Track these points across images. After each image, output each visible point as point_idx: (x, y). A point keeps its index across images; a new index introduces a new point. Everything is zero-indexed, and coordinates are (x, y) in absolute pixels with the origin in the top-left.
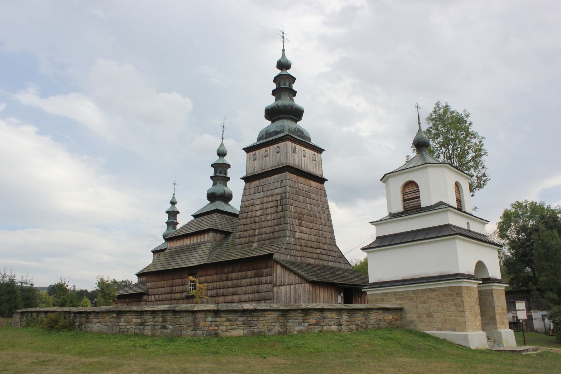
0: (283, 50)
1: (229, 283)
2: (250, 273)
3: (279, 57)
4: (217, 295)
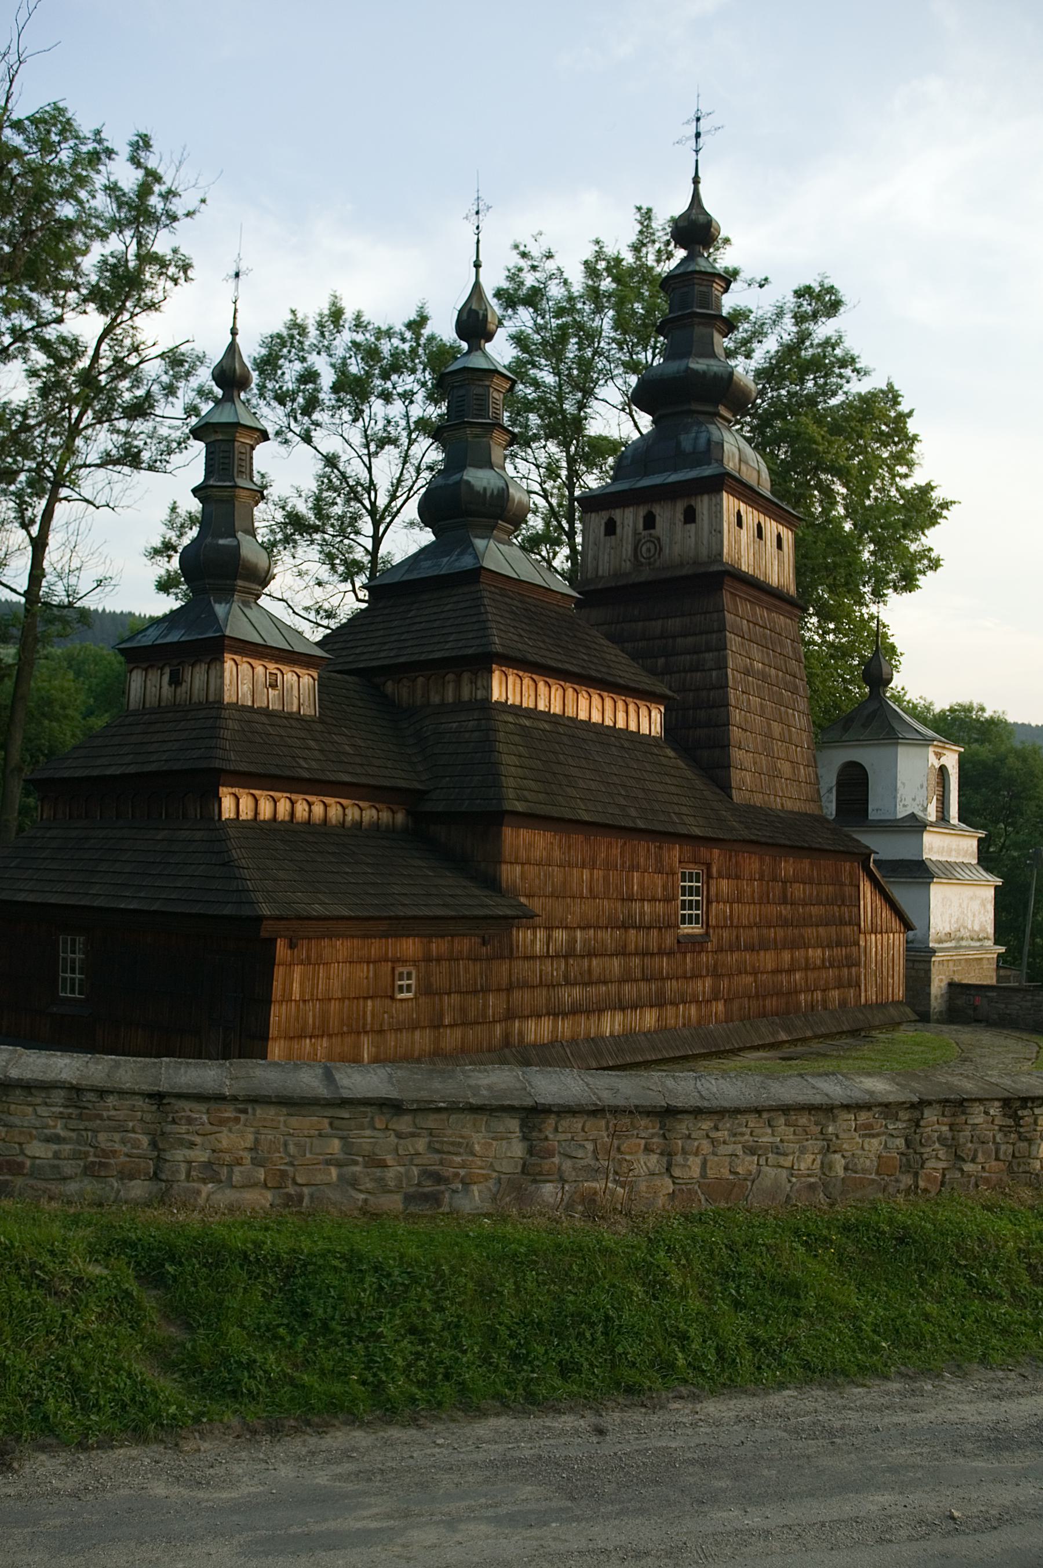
0: (696, 181)
1: (786, 911)
4: (764, 946)
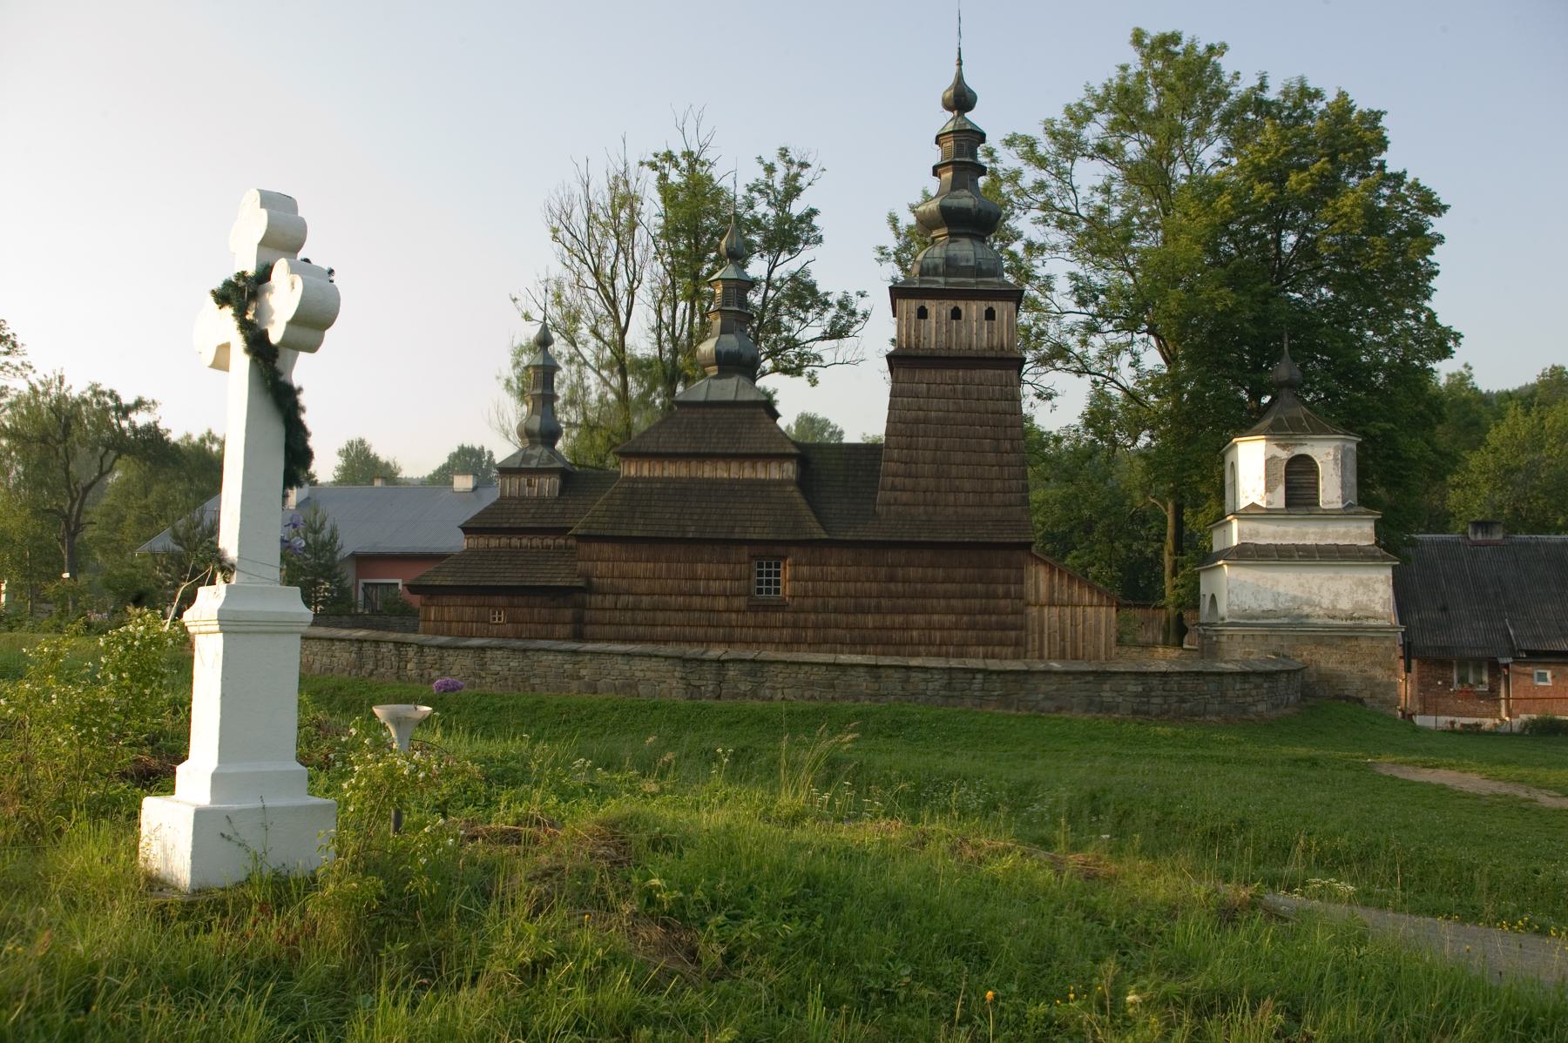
0: (960, 63)
2: (960, 573)
3: (950, 80)
